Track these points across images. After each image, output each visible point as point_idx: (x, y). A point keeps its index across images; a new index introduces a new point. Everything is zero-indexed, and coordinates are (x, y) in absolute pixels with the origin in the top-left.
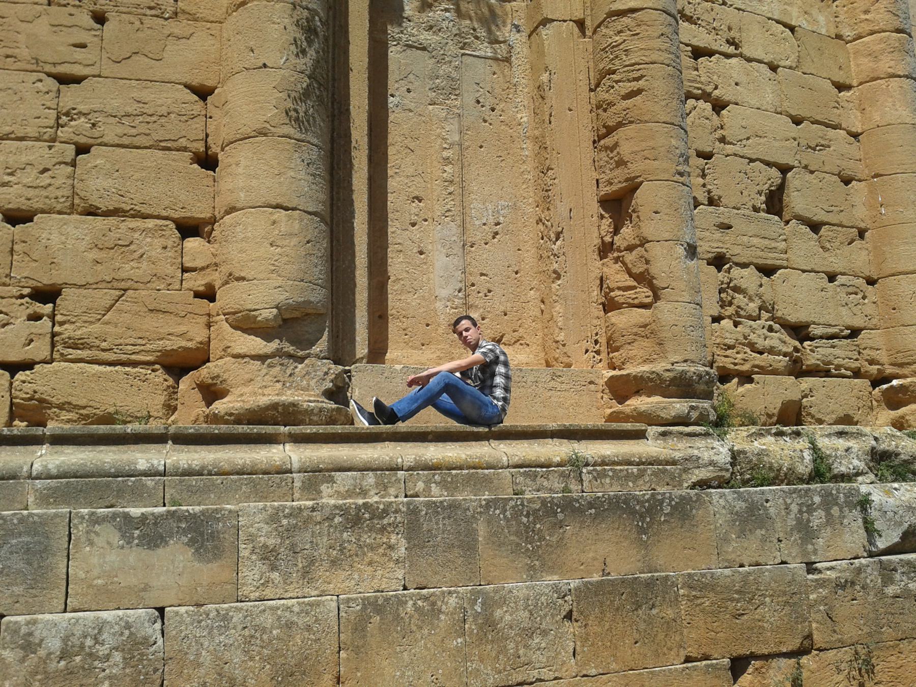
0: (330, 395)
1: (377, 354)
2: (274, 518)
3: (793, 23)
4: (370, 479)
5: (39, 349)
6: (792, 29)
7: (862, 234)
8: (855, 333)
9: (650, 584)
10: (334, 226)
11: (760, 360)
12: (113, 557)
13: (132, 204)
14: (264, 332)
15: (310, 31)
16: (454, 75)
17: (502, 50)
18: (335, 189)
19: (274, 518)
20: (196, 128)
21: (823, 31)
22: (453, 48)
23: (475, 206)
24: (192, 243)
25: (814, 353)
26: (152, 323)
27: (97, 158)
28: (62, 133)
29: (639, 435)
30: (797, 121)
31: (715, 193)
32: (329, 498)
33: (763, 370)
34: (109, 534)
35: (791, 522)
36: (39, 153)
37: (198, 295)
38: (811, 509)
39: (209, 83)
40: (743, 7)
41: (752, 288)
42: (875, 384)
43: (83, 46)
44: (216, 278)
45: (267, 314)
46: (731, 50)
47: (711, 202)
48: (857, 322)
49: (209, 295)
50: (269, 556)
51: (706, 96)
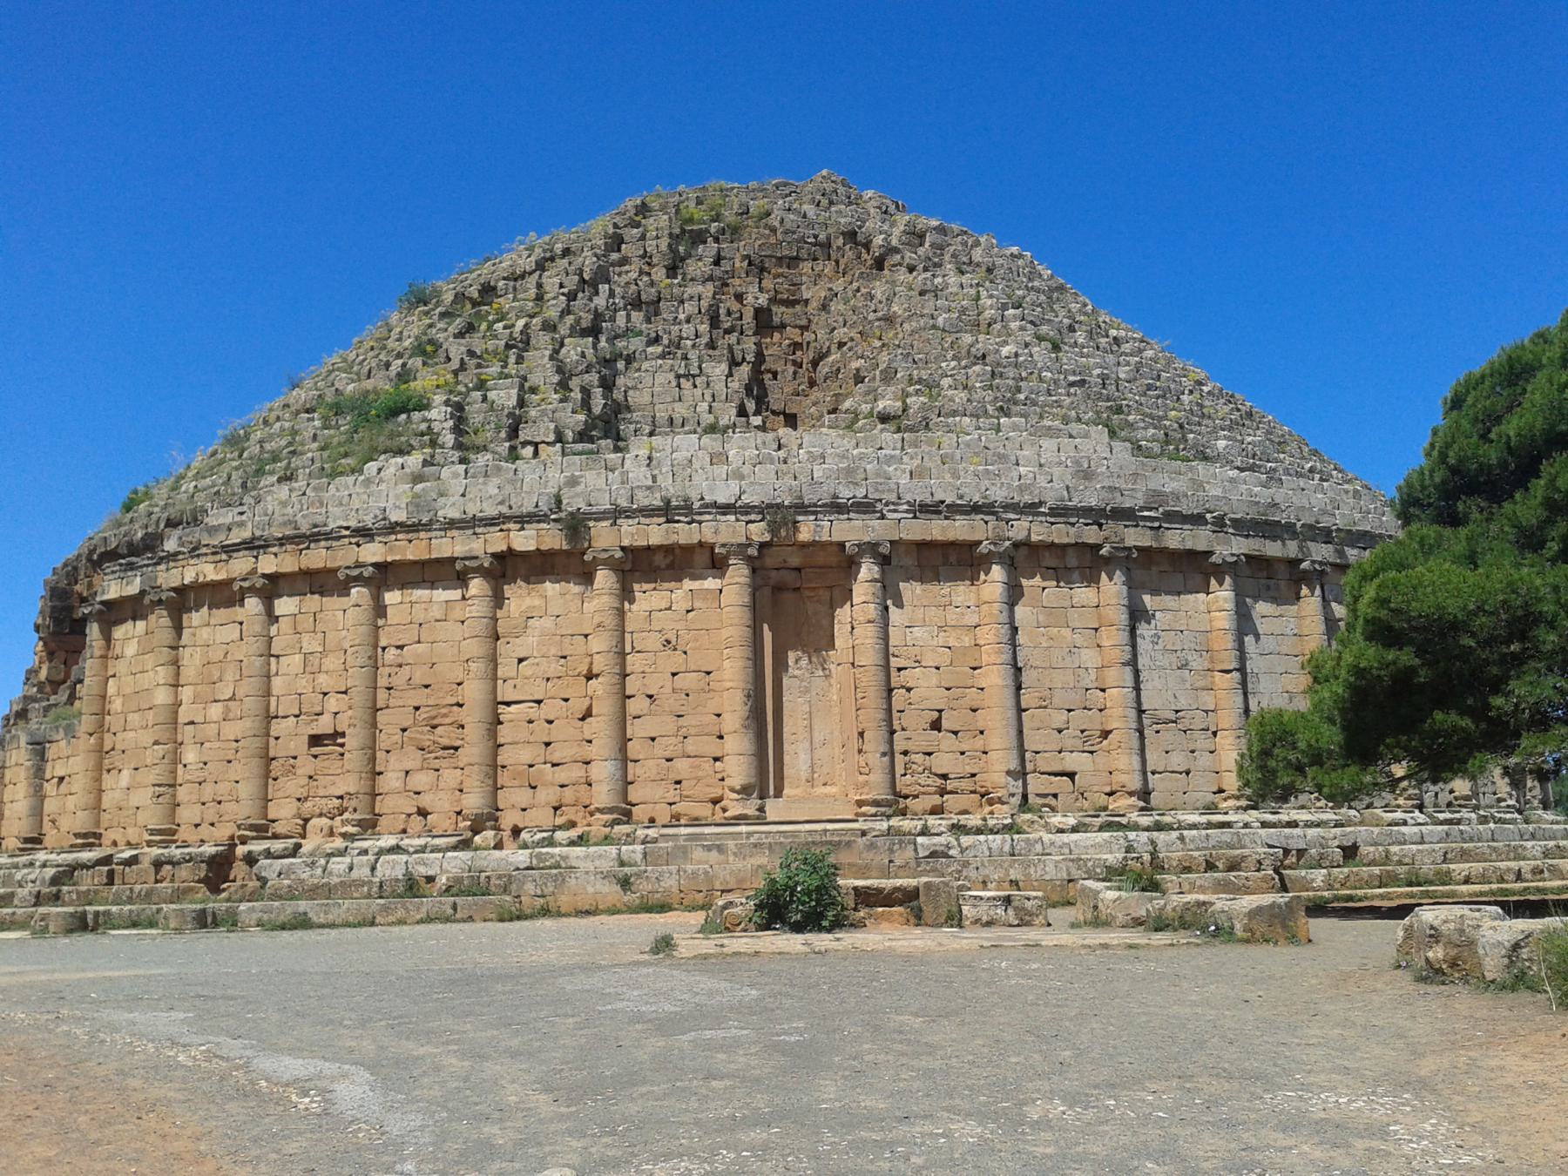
0: (759, 810)
1: (778, 794)
5: (677, 799)
7: (982, 732)
8: (973, 775)
11: (922, 789)
14: (738, 792)
15: (748, 696)
17: (827, 672)
20: (717, 728)
22: (807, 675)
23: (816, 734)
24: (718, 763)
25: (950, 785)
26: (708, 790)
29: (857, 821)
30: (948, 689)
32: (752, 840)
33: (924, 793)
34: (700, 849)
36: (673, 740)
41: (920, 762)
42: (983, 796)
44: (725, 774)
45: (738, 787)
47: (903, 729)
48: (974, 771)
49: (723, 780)
50: (735, 854)
51: (903, 687)
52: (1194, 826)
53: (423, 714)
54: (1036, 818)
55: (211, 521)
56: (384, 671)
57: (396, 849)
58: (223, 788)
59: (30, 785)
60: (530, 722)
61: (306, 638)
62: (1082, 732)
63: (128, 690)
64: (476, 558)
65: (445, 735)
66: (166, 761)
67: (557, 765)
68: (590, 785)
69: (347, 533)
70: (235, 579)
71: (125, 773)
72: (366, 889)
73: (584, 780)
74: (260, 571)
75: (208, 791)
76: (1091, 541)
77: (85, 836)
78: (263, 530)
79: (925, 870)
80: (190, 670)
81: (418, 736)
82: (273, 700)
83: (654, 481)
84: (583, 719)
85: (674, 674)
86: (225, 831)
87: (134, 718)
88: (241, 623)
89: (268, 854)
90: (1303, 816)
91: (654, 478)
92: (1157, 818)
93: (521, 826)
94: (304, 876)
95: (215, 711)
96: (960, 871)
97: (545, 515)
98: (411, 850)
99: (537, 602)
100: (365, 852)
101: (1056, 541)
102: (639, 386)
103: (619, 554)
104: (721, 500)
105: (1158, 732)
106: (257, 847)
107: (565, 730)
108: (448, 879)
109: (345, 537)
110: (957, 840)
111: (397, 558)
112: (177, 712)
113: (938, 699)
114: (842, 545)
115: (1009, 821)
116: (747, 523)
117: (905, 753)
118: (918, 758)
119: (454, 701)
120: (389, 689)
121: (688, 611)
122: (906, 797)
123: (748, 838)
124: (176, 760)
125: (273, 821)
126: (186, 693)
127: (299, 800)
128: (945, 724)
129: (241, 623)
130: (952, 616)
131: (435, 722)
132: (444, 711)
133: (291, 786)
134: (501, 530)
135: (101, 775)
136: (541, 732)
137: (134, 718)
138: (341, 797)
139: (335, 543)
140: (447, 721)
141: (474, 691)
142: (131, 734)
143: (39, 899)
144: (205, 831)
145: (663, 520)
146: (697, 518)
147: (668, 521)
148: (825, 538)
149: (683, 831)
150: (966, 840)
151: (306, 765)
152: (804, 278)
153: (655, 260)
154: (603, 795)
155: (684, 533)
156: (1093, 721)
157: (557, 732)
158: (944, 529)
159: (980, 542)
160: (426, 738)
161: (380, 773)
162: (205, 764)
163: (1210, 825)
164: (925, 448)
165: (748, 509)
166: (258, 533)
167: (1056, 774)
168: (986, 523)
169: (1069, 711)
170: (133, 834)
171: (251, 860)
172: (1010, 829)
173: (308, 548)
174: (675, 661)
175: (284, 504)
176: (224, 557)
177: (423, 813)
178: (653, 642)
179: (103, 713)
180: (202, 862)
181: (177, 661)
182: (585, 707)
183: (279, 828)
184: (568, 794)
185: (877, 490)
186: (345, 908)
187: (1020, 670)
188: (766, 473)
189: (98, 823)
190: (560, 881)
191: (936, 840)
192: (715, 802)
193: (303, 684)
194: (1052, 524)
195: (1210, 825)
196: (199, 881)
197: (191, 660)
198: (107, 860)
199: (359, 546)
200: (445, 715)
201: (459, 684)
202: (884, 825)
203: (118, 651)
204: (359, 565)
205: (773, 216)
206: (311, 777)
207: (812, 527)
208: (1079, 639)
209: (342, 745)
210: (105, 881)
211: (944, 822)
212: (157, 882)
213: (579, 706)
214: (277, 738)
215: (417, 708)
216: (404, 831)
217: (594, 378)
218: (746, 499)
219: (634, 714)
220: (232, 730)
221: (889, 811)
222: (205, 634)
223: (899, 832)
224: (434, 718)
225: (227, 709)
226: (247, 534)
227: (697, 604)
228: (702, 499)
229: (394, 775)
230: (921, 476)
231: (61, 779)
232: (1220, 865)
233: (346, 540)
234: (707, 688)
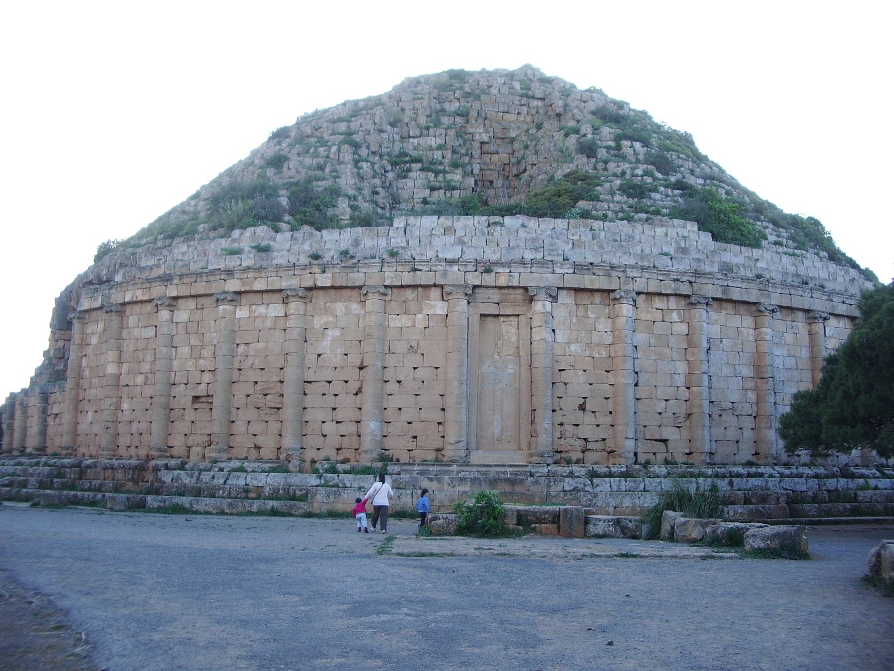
2: (449, 478)
4: (467, 473)
8: (604, 440)
9: (512, 493)
12: (426, 483)
19: (449, 478)
21: (604, 356)
25: (590, 446)
27: (422, 411)
35: (545, 484)
37: (441, 437)
38: (550, 482)
50: (449, 484)
52: (739, 475)
53: (259, 387)
54: (642, 468)
55: (143, 263)
56: (237, 359)
57: (242, 470)
58: (143, 426)
59: (39, 418)
60: (324, 395)
61: (192, 336)
62: (674, 414)
63: (93, 365)
64: (294, 290)
65: (272, 401)
66: (112, 408)
67: (340, 422)
68: (359, 436)
69: (218, 273)
70: (153, 299)
71: (90, 413)
72: (221, 492)
73: (355, 433)
74: (167, 295)
75: (135, 427)
76: (684, 293)
77: (67, 448)
78: (171, 270)
79: (570, 499)
80: (126, 355)
81: (256, 400)
82: (173, 375)
83: (408, 244)
84: (356, 394)
85: (415, 368)
86: (143, 452)
87: (95, 381)
88: (156, 326)
89: (167, 467)
90: (806, 471)
91: (408, 242)
92: (717, 469)
93: (316, 459)
94: (187, 481)
95: (140, 379)
96: (590, 500)
97: (338, 264)
98: (249, 470)
99: (331, 319)
100: (221, 470)
101: (663, 292)
102: (405, 187)
103: (382, 290)
104: (450, 256)
105: (720, 416)
106: (161, 462)
107: (346, 402)
108: (270, 489)
109: (217, 275)
110: (592, 481)
111: (248, 289)
112: (119, 378)
113: (585, 391)
114: (526, 289)
115: (624, 469)
117: (561, 424)
118: (569, 429)
119: (278, 380)
120: (240, 370)
122: (561, 452)
123: (457, 474)
124: (119, 408)
125: (171, 447)
126: (125, 367)
127: (186, 435)
128: (588, 407)
129: (156, 326)
130: (595, 338)
131: (266, 392)
132: (272, 385)
133: (181, 427)
134: (310, 273)
135: (77, 414)
136: (330, 401)
137: (95, 381)
138: (210, 435)
139: (211, 278)
140: (273, 391)
141: (291, 374)
142: (93, 391)
143: (42, 485)
144: (133, 451)
146: (433, 268)
148: (515, 284)
149: (416, 468)
150: (595, 480)
151: (190, 415)
152: (513, 125)
153: (420, 112)
154: (367, 443)
155: (423, 278)
156: (682, 410)
157: (338, 402)
158: (592, 281)
160: (261, 402)
161: (233, 422)
162: (134, 410)
163: (749, 475)
164: (582, 229)
165: (466, 263)
166: (167, 272)
167: (656, 440)
168: (619, 278)
169: (666, 400)
170: (93, 450)
171: (156, 469)
172: (626, 475)
173: (196, 282)
174: (416, 360)
175: (183, 254)
176: (148, 285)
177: (258, 447)
178: (401, 347)
179: (79, 376)
180: (130, 469)
181: (120, 348)
182: (357, 387)
183: (175, 452)
184: (346, 442)
185: (550, 254)
186: (206, 503)
187: (636, 373)
188: (479, 241)
189: (75, 443)
190: (337, 494)
191: (577, 479)
192: (438, 450)
193: (190, 365)
194: (661, 281)
195: (749, 475)
196: (129, 480)
197: (129, 346)
198: (79, 465)
199: (225, 280)
200: (273, 388)
201: (282, 369)
202: (546, 470)
203: (88, 340)
204: (225, 292)
205: (494, 87)
206: (193, 422)
207: (508, 277)
208: (675, 356)
209: (212, 403)
210: (77, 476)
211: (583, 469)
212: (105, 479)
213: (354, 386)
214: (175, 397)
215: (256, 383)
216: (246, 458)
217: (377, 181)
218: (466, 257)
220: (148, 391)
221: (550, 461)
222: (136, 332)
223: (554, 475)
224: (267, 389)
225: (147, 378)
226: (161, 272)
227: (431, 324)
228: (437, 256)
229: (240, 423)
230: (579, 246)
231: (57, 414)
232: (753, 500)
233: (218, 277)
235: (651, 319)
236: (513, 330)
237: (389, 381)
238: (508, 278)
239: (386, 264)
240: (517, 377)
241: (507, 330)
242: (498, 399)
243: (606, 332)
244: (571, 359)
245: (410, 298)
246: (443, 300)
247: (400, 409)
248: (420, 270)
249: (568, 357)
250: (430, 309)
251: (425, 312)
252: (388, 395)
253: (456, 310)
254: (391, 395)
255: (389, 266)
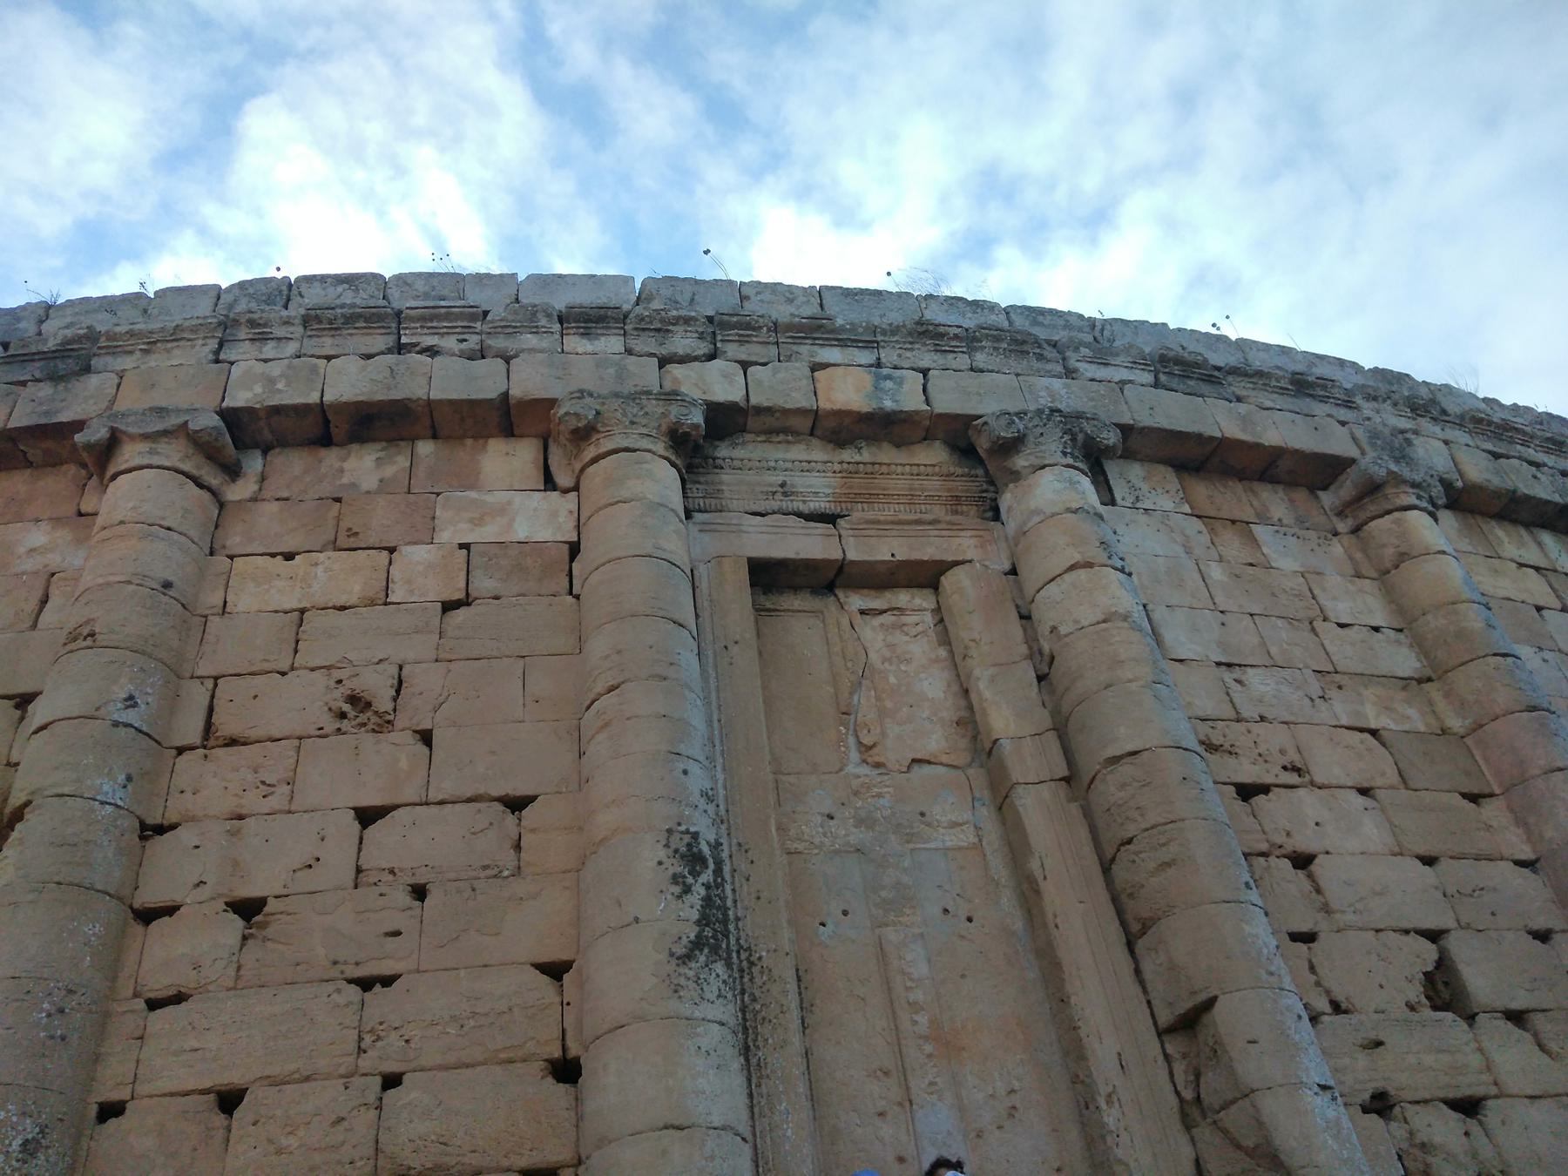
3: (1373, 726)
6: (1374, 733)
10: (758, 1140)
13: (458, 1156)
16: (906, 879)
18: (754, 1081)
21: (1422, 728)
28: (365, 1063)
30: (1429, 861)
31: (1340, 997)
39: (563, 956)
40: (1292, 719)
43: (397, 933)
46: (1292, 778)
47: (1337, 1008)
85: (367, 817)
116: (663, 362)
121: (448, 607)
145: (380, 342)
146: (498, 343)
147: (400, 348)
158: (1245, 421)
159: (1353, 461)
168: (1343, 423)
194: (1496, 456)
219: (159, 985)
227: (483, 584)
234: (507, 858)
235: (1524, 597)
236: (921, 648)
237: (171, 910)
238: (870, 388)
239: (243, 333)
240: (999, 868)
241: (891, 646)
242: (918, 995)
243: (1376, 629)
244: (1274, 739)
245: (369, 482)
246: (549, 483)
247: (229, 1101)
248: (432, 351)
249: (1259, 729)
250: (478, 522)
251: (451, 534)
252: (154, 1005)
253: (625, 494)
254: (179, 998)
255: (262, 339)
